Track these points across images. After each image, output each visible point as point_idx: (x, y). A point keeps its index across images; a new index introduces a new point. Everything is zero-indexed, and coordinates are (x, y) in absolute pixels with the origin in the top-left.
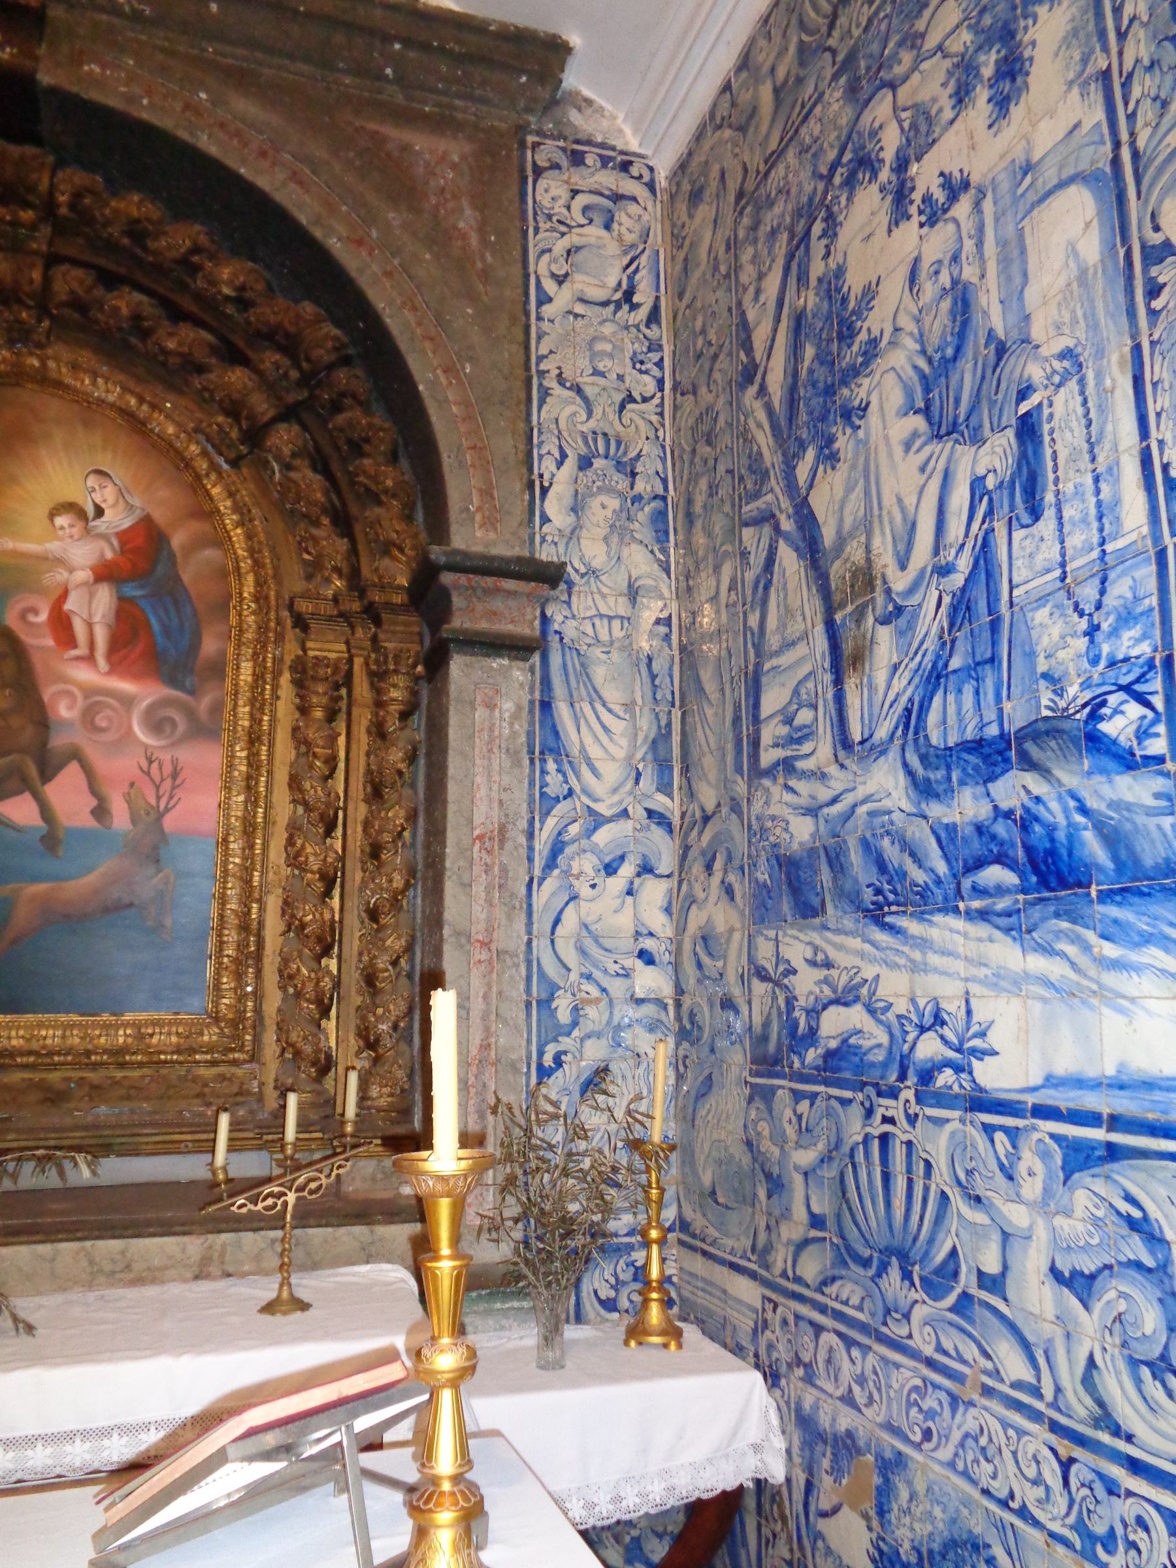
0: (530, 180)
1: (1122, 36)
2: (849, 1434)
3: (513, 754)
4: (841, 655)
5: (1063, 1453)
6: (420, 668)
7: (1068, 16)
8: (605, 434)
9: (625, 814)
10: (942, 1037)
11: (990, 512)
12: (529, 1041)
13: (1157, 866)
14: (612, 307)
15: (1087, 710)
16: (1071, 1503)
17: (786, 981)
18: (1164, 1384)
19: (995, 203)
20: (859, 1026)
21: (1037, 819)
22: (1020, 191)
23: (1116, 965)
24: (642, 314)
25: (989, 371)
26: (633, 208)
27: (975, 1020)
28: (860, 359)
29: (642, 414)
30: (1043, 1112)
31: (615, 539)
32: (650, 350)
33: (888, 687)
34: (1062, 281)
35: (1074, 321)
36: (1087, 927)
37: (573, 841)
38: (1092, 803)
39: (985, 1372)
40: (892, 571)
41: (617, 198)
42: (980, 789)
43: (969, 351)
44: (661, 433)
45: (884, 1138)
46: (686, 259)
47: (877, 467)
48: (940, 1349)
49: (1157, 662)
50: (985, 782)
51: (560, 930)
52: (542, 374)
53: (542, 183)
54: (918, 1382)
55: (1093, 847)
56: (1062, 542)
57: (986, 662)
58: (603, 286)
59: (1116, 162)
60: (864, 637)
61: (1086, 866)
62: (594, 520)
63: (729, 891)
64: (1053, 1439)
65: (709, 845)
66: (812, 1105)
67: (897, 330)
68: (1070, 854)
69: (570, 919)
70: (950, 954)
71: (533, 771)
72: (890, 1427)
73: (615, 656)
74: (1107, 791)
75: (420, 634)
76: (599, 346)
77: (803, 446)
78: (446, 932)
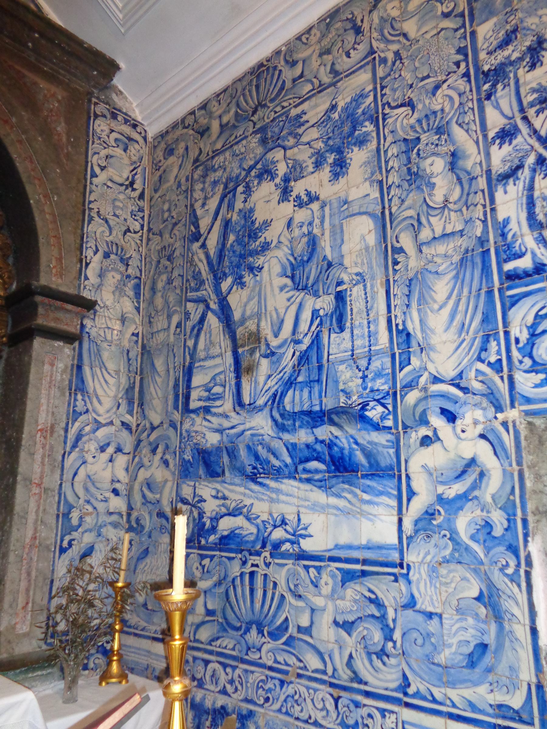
0: (92, 118)
1: (388, 172)
2: (223, 707)
3: (61, 390)
4: (241, 367)
5: (335, 695)
6: (4, 339)
7: (367, 155)
9: (111, 423)
10: (285, 530)
11: (321, 324)
12: (57, 535)
13: (386, 467)
14: (124, 187)
16: (339, 714)
17: (199, 505)
18: (382, 661)
20: (241, 525)
21: (335, 445)
23: (369, 502)
24: (136, 194)
25: (323, 271)
26: (136, 146)
27: (302, 522)
28: (259, 249)
29: (133, 238)
30: (332, 559)
31: (117, 293)
33: (265, 384)
34: (358, 247)
37: (87, 434)
38: (360, 441)
39: (301, 668)
40: (270, 337)
41: (130, 139)
42: (309, 431)
43: (315, 260)
45: (252, 574)
46: (160, 177)
47: (265, 294)
48: (276, 661)
50: (312, 428)
51: (76, 478)
52: (90, 209)
53: (97, 122)
54: (264, 678)
55: (360, 457)
56: (353, 342)
57: (315, 381)
58: (121, 177)
59: (383, 213)
60: (254, 361)
63: (166, 463)
64: (330, 690)
66: (211, 561)
67: (279, 242)
68: (350, 459)
69: (82, 473)
70: (291, 495)
71: (70, 399)
72: (247, 700)
73: (113, 348)
74: (367, 437)
75: (7, 322)
77: (225, 275)
78: (19, 478)
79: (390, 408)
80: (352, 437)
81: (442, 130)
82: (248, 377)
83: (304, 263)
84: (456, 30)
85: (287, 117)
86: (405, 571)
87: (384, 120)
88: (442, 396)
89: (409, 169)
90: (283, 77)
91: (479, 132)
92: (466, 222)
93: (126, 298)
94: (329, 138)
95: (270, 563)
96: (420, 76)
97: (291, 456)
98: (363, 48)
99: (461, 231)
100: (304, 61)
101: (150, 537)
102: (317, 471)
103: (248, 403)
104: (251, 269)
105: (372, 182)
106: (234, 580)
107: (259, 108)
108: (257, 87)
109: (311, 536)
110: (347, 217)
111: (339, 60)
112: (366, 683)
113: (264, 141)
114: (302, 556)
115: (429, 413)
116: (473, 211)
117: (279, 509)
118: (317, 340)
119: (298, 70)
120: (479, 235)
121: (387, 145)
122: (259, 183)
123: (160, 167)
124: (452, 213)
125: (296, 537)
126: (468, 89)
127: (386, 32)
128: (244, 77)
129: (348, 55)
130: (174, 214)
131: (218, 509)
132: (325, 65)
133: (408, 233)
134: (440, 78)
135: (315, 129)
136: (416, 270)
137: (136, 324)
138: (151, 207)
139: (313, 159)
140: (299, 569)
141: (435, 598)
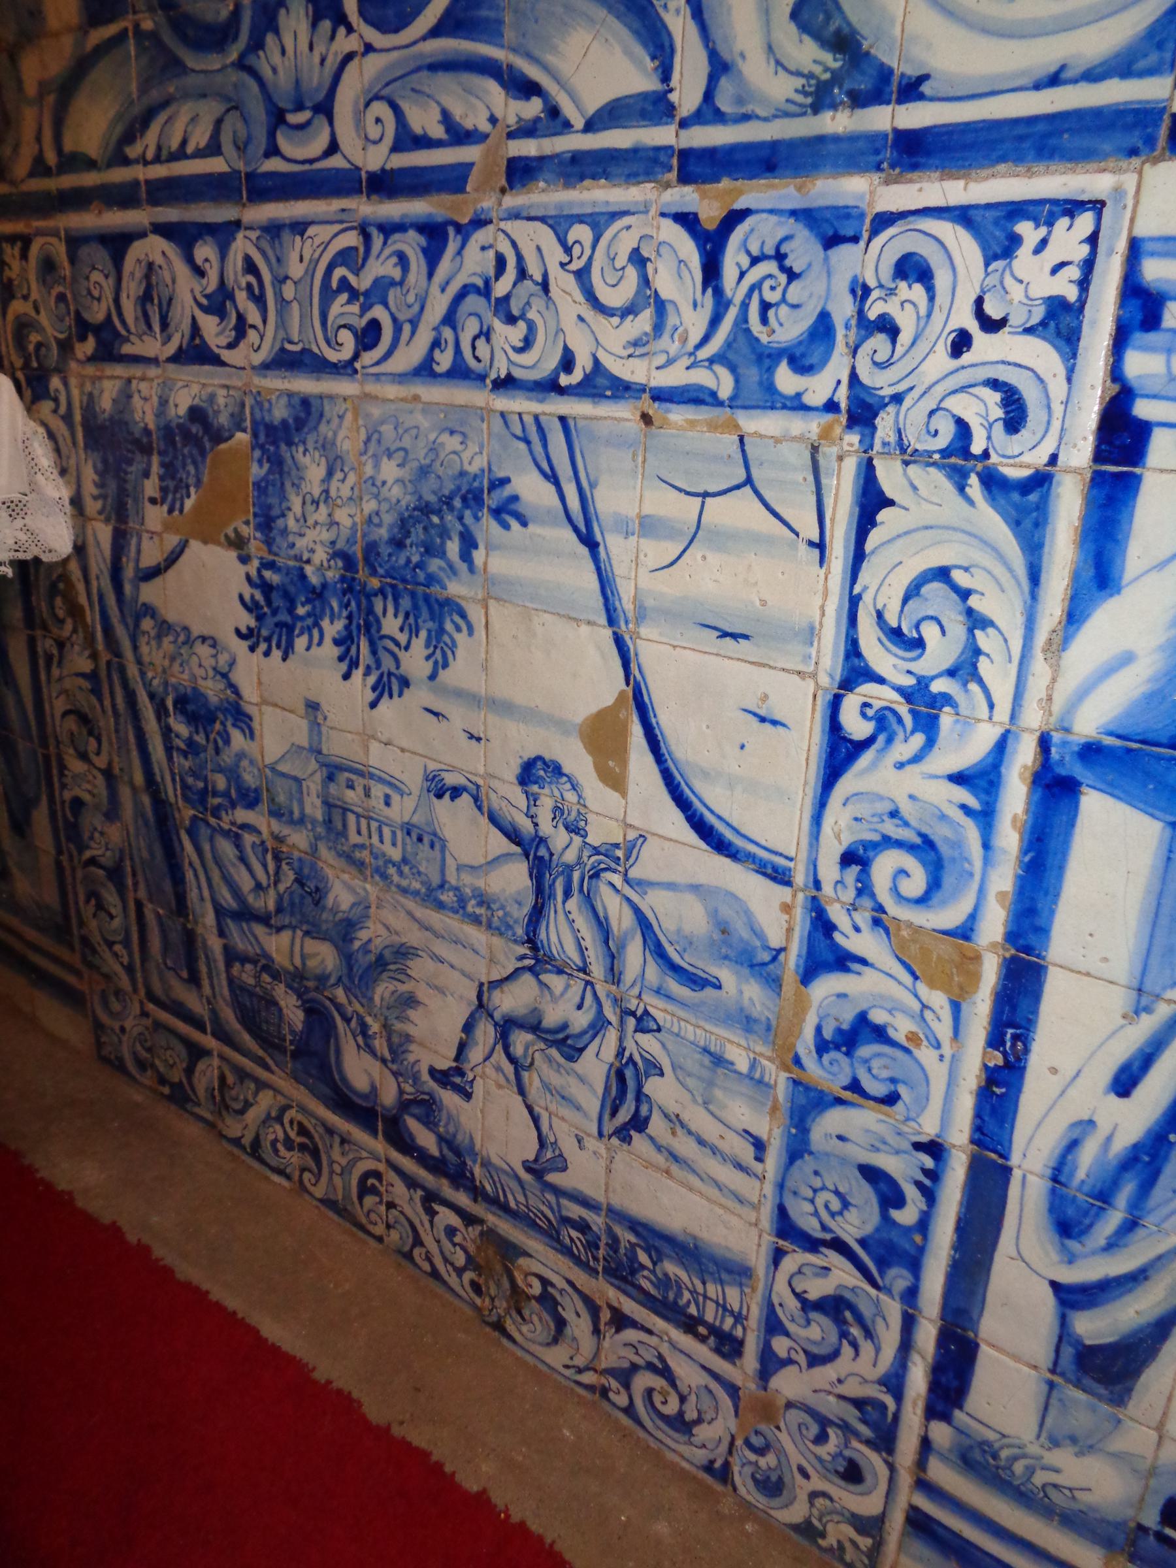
2: (196, 414)
16: (721, 304)
39: (528, 130)
48: (407, 140)
54: (351, 239)
64: (686, 197)
72: (288, 361)
112: (912, 90)
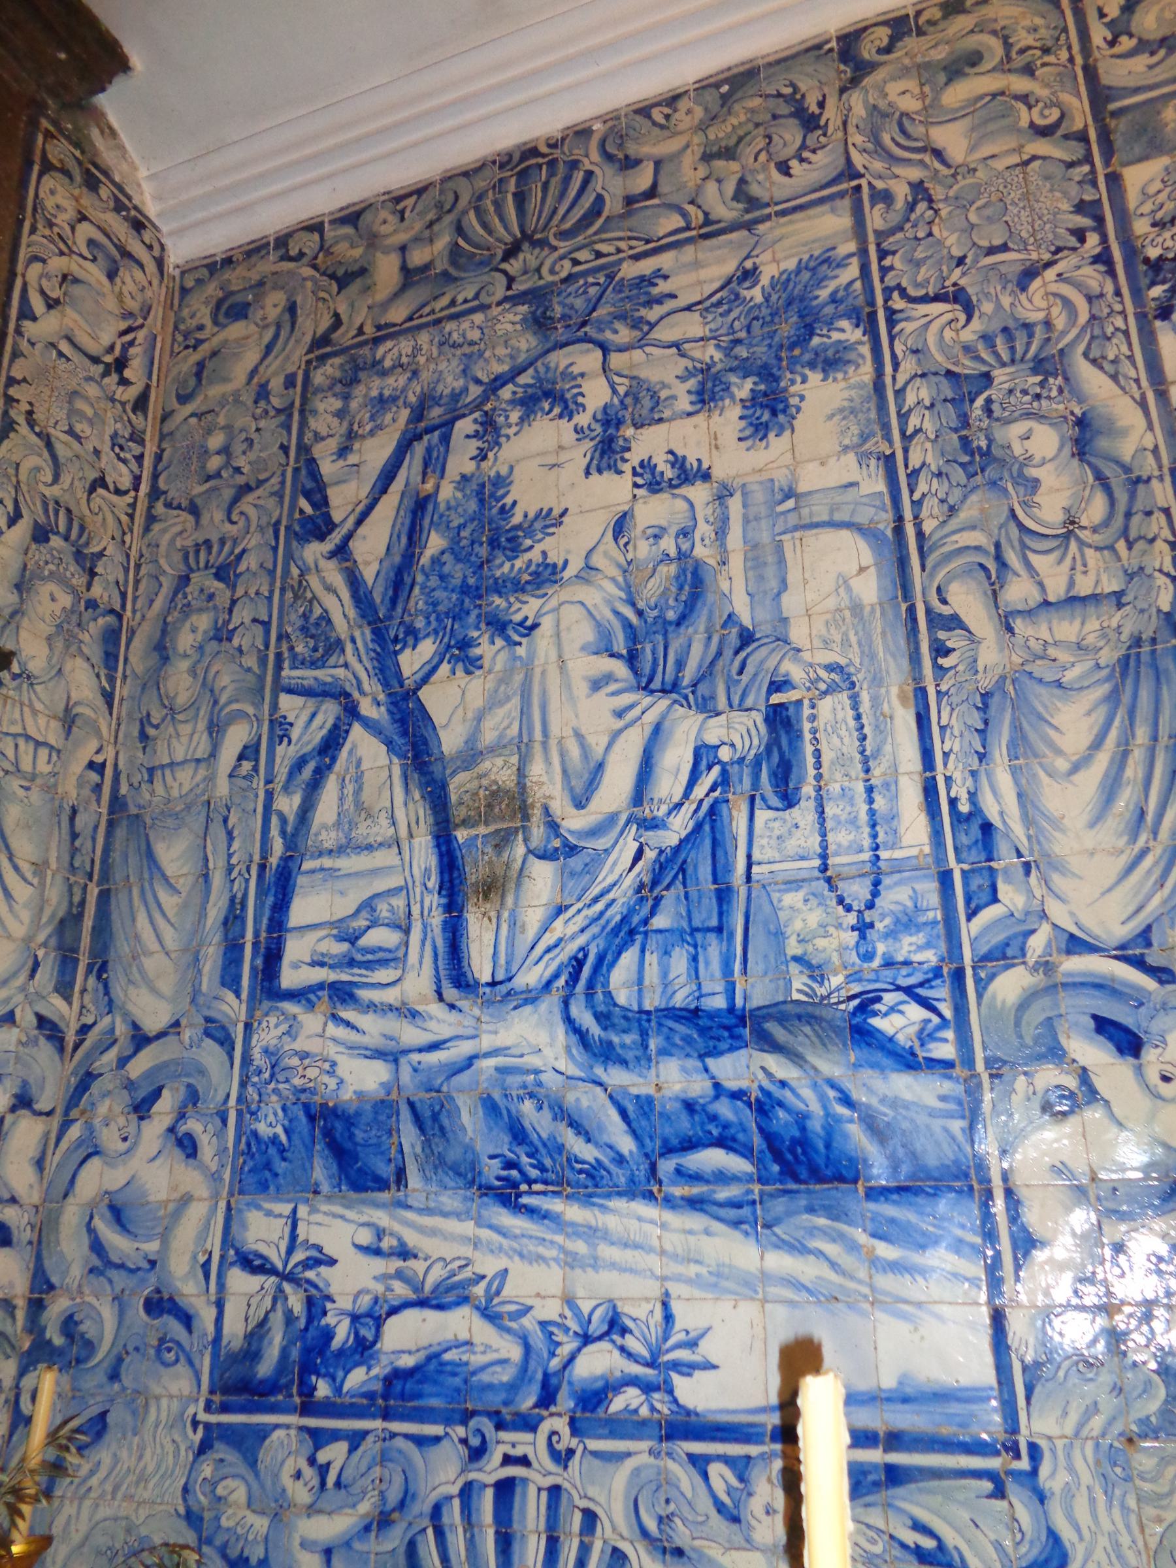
0: (36, 168)
7: (846, 394)
8: (69, 511)
10: (622, 1349)
11: (724, 781)
15: (856, 1002)
17: (310, 1274)
19: (745, 506)
20: (463, 1336)
21: (781, 1104)
22: (780, 509)
23: (895, 1267)
24: (131, 393)
25: (728, 653)
26: (138, 274)
27: (679, 1325)
28: (526, 577)
31: (59, 644)
32: (131, 439)
33: (545, 929)
34: (831, 603)
35: (845, 643)
36: (850, 1223)
40: (560, 806)
41: (126, 254)
44: (128, 538)
45: (505, 1489)
46: (201, 365)
47: (544, 693)
49: (945, 970)
53: (48, 182)
56: (824, 835)
57: (709, 930)
58: (95, 338)
59: (899, 530)
60: (508, 865)
61: (850, 1159)
62: (40, 610)
63: (188, 1146)
65: (149, 1074)
66: (352, 1449)
68: (828, 1146)
70: (637, 1246)
73: (35, 796)
76: (80, 405)
77: (413, 636)
79: (947, 1011)
80: (833, 1086)
81: (1048, 366)
82: (490, 908)
83: (665, 627)
84: (1071, 165)
85: (611, 277)
86: (1024, 1464)
87: (891, 323)
88: (1098, 986)
89: (965, 442)
90: (597, 185)
91: (1144, 383)
92: (1130, 576)
93: (79, 661)
94: (738, 342)
95: (571, 1452)
96: (985, 243)
97: (634, 1133)
98: (824, 163)
99: (1118, 596)
100: (658, 164)
101: (114, 1376)
102: (722, 1177)
103: (486, 977)
104: (499, 626)
105: (863, 458)
106: (437, 1511)
107: (526, 246)
108: (521, 199)
109: (710, 1366)
110: (796, 528)
111: (761, 177)
113: (540, 323)
114: (683, 1427)
115: (1061, 1028)
116: (1144, 552)
117: (594, 1289)
118: (711, 821)
119: (642, 180)
120: (1166, 608)
121: (902, 378)
122: (522, 419)
123: (200, 342)
124: (1089, 552)
125: (659, 1370)
126: (1109, 288)
127: (886, 139)
128: (478, 170)
129: (784, 169)
130: (241, 462)
131: (379, 1288)
132: (719, 181)
133: (973, 585)
134: (1034, 256)
135: (696, 316)
136: (999, 671)
137: (100, 737)
138: (162, 437)
139: (692, 383)
140: (672, 1465)
141: (1125, 1540)
